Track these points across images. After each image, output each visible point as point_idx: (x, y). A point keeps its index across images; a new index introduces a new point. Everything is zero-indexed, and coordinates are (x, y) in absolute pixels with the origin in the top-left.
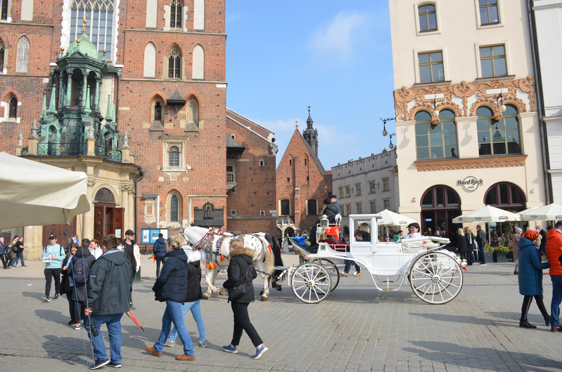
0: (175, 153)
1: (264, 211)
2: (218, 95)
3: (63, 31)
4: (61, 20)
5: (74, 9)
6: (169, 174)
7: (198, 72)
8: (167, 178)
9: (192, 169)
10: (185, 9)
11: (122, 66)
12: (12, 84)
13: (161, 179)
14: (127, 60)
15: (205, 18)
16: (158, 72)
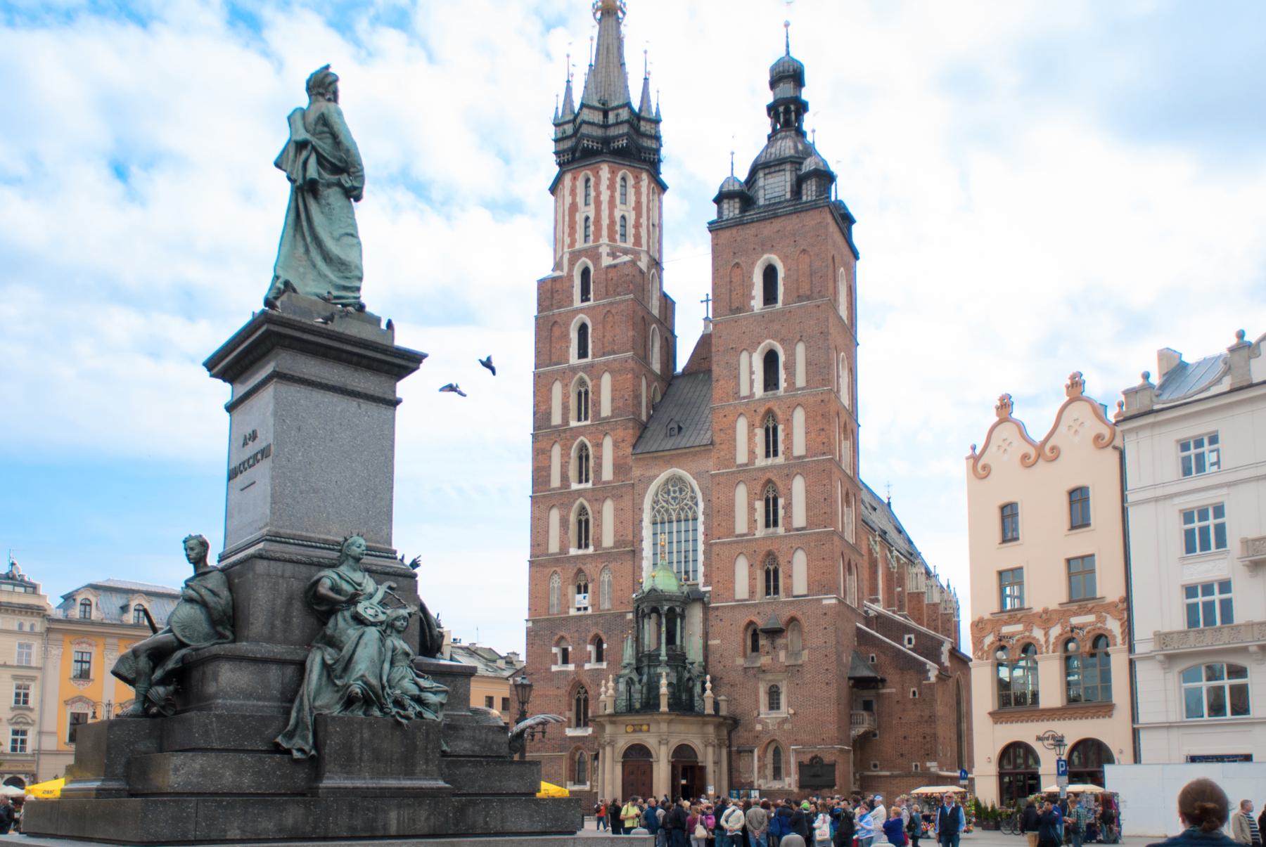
0: (774, 694)
1: (919, 764)
2: (825, 614)
3: (645, 554)
4: (642, 541)
5: (655, 523)
6: (768, 721)
7: (800, 586)
8: (765, 724)
9: (794, 714)
10: (781, 502)
11: (709, 588)
12: (597, 624)
13: (759, 727)
14: (715, 580)
15: (807, 510)
16: (752, 593)
